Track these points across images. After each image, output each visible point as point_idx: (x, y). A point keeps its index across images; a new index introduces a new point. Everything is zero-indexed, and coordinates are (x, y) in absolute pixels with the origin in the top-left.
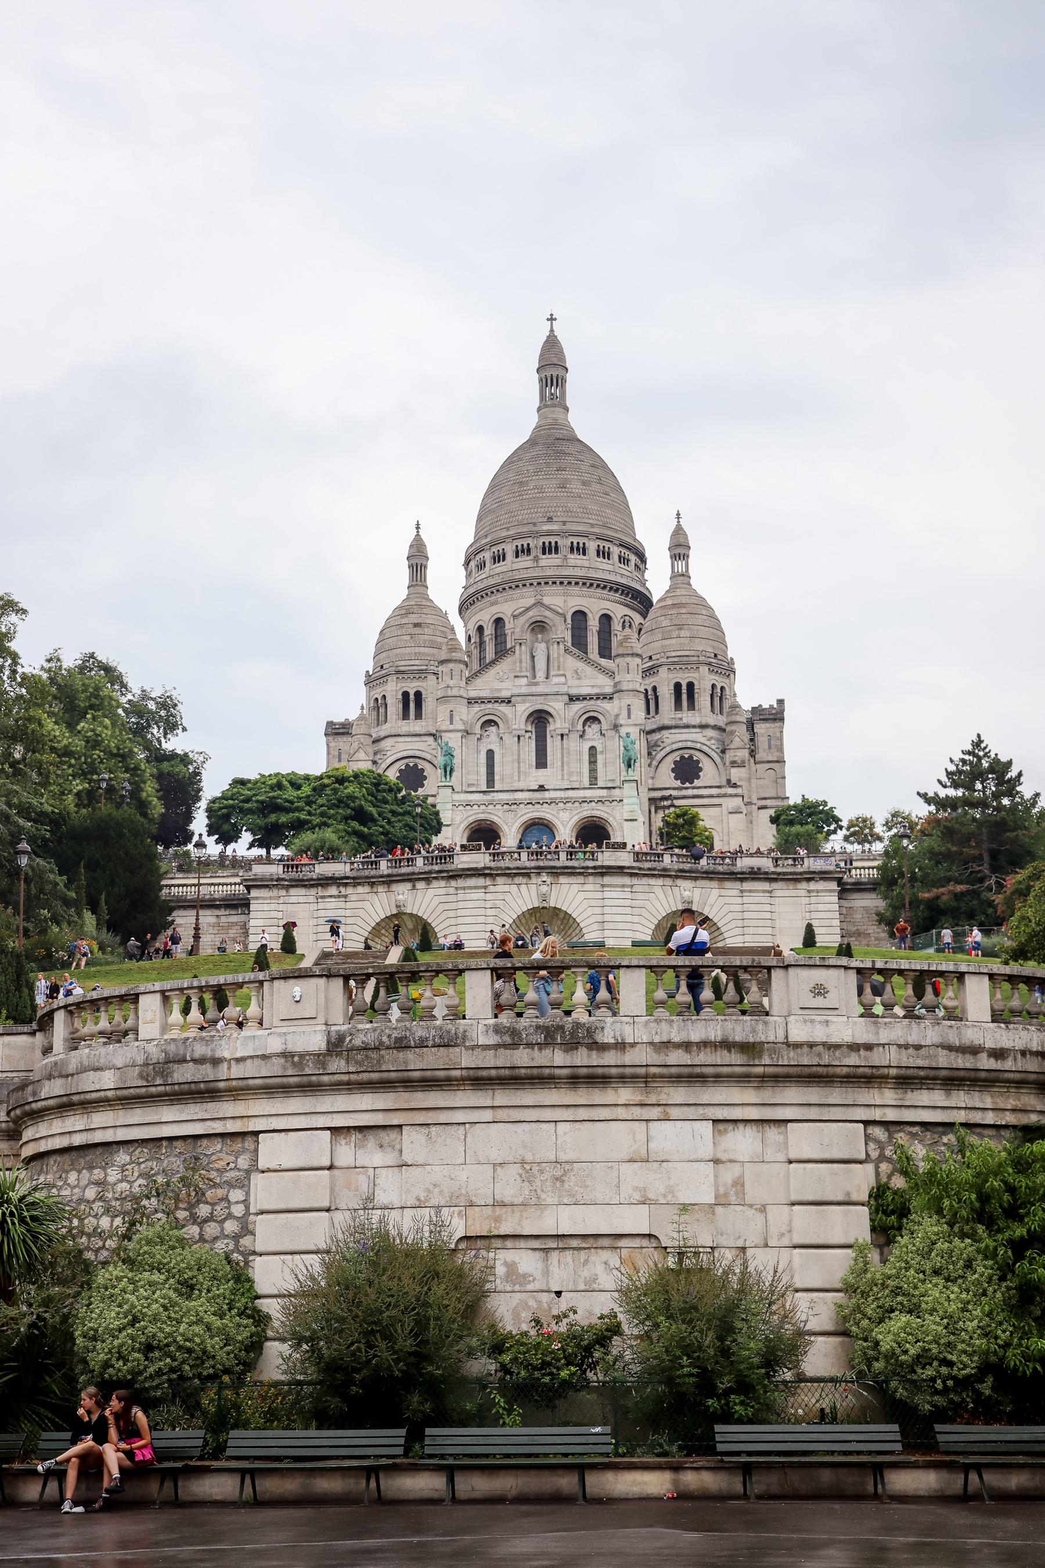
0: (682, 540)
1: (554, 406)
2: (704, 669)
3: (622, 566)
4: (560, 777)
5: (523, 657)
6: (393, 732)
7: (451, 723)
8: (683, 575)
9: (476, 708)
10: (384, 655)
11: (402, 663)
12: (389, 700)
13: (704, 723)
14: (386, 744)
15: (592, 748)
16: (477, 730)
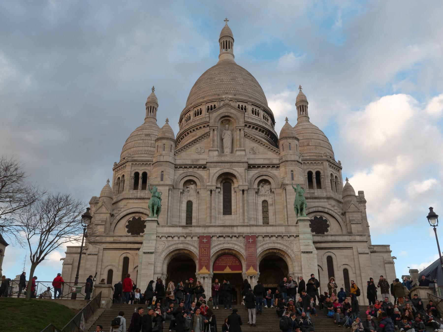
0: (303, 98)
1: (228, 53)
2: (326, 164)
3: (265, 121)
4: (241, 221)
5: (215, 138)
6: (126, 197)
7: (162, 180)
8: (306, 116)
9: (181, 171)
10: (126, 152)
11: (136, 155)
12: (126, 177)
13: (328, 196)
14: (121, 204)
15: (265, 202)
16: (181, 185)
